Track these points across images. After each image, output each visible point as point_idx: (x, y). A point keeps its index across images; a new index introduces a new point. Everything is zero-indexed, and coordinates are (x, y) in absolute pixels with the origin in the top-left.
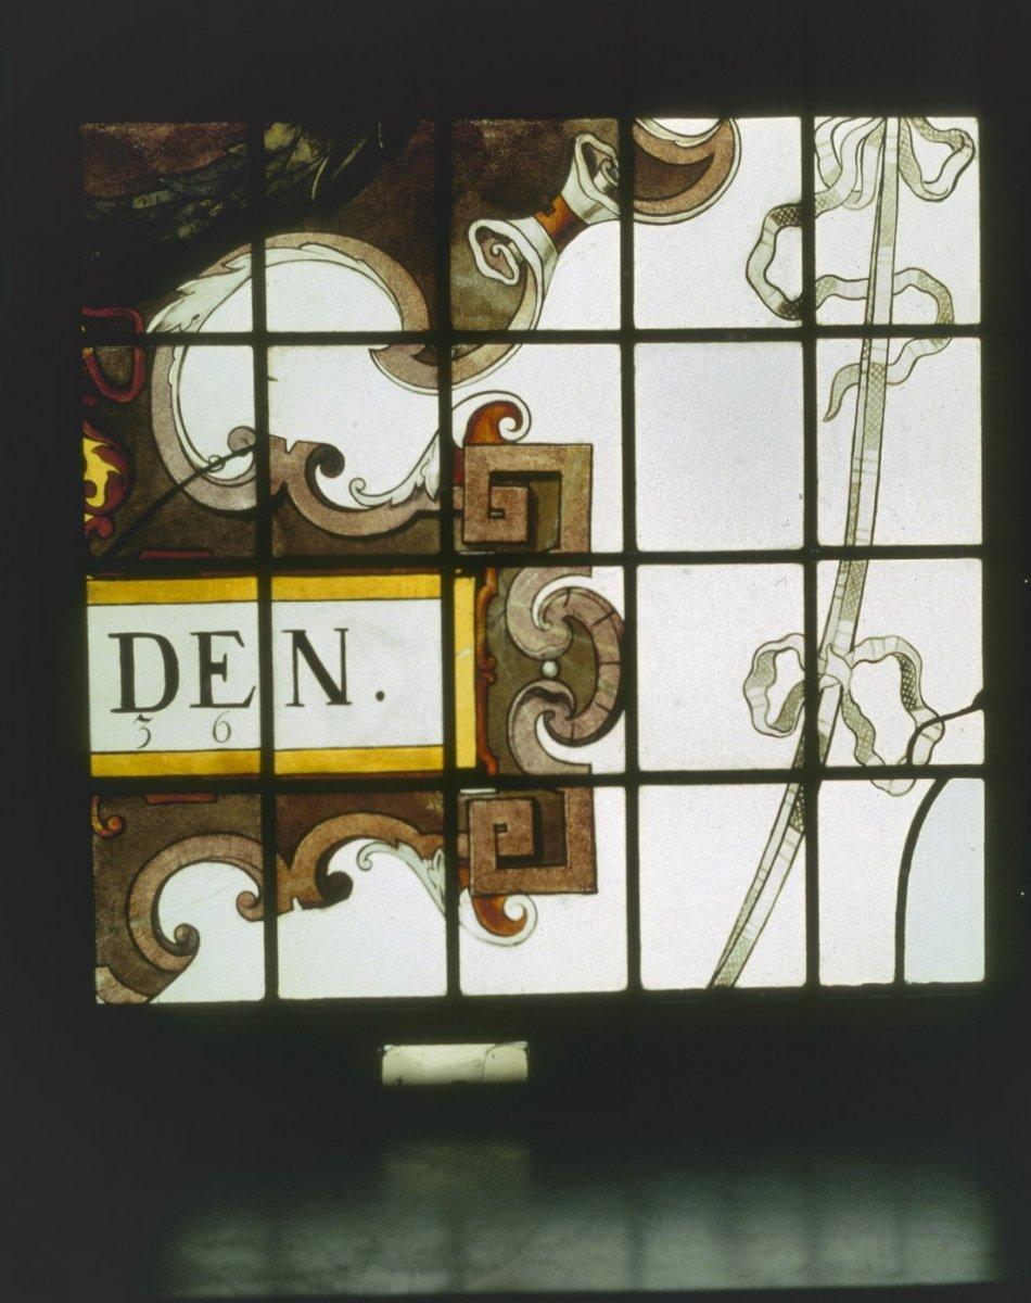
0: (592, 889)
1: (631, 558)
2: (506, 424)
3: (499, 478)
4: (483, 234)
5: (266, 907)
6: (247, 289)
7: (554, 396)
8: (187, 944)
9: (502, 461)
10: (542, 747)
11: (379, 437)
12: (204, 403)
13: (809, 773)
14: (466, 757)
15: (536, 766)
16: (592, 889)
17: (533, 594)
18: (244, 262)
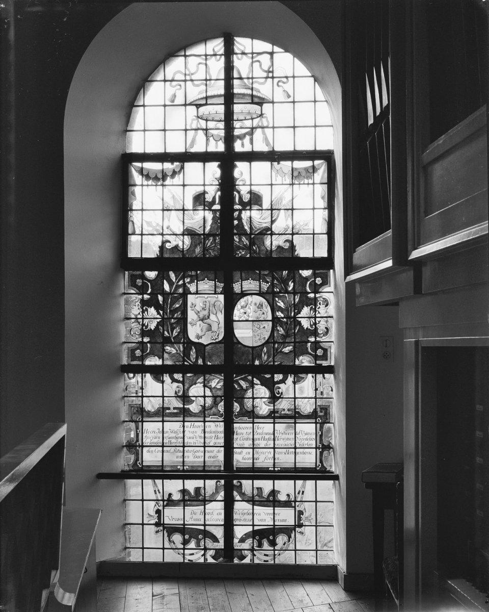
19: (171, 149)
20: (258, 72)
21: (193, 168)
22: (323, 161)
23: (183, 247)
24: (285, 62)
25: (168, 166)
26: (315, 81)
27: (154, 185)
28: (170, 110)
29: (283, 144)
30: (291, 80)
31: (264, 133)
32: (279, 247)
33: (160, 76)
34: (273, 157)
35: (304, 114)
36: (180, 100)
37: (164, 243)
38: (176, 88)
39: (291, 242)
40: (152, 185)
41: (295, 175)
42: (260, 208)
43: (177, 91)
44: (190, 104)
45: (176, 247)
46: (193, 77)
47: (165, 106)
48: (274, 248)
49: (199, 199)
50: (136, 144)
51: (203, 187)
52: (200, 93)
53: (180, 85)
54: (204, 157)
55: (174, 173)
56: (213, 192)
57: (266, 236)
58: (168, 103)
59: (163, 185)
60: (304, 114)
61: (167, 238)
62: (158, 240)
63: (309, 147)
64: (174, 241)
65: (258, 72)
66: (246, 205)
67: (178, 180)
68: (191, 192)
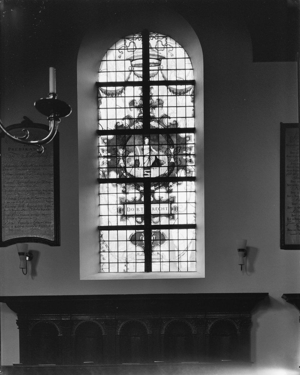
10: (173, 212)
12: (157, 196)
17: (173, 205)
19: (119, 80)
21: (129, 90)
22: (191, 86)
23: (125, 125)
25: (119, 88)
26: (185, 51)
28: (118, 62)
29: (172, 77)
31: (161, 73)
32: (170, 123)
34: (167, 83)
35: (181, 64)
36: (123, 58)
37: (117, 123)
38: (121, 53)
39: (176, 122)
40: (110, 97)
41: (177, 94)
44: (127, 60)
45: (123, 125)
46: (128, 48)
47: (116, 60)
50: (102, 78)
51: (133, 98)
52: (132, 54)
54: (134, 84)
55: (121, 92)
56: (138, 101)
58: (118, 59)
59: (116, 97)
61: (118, 121)
64: (121, 122)
67: (123, 95)
68: (128, 100)
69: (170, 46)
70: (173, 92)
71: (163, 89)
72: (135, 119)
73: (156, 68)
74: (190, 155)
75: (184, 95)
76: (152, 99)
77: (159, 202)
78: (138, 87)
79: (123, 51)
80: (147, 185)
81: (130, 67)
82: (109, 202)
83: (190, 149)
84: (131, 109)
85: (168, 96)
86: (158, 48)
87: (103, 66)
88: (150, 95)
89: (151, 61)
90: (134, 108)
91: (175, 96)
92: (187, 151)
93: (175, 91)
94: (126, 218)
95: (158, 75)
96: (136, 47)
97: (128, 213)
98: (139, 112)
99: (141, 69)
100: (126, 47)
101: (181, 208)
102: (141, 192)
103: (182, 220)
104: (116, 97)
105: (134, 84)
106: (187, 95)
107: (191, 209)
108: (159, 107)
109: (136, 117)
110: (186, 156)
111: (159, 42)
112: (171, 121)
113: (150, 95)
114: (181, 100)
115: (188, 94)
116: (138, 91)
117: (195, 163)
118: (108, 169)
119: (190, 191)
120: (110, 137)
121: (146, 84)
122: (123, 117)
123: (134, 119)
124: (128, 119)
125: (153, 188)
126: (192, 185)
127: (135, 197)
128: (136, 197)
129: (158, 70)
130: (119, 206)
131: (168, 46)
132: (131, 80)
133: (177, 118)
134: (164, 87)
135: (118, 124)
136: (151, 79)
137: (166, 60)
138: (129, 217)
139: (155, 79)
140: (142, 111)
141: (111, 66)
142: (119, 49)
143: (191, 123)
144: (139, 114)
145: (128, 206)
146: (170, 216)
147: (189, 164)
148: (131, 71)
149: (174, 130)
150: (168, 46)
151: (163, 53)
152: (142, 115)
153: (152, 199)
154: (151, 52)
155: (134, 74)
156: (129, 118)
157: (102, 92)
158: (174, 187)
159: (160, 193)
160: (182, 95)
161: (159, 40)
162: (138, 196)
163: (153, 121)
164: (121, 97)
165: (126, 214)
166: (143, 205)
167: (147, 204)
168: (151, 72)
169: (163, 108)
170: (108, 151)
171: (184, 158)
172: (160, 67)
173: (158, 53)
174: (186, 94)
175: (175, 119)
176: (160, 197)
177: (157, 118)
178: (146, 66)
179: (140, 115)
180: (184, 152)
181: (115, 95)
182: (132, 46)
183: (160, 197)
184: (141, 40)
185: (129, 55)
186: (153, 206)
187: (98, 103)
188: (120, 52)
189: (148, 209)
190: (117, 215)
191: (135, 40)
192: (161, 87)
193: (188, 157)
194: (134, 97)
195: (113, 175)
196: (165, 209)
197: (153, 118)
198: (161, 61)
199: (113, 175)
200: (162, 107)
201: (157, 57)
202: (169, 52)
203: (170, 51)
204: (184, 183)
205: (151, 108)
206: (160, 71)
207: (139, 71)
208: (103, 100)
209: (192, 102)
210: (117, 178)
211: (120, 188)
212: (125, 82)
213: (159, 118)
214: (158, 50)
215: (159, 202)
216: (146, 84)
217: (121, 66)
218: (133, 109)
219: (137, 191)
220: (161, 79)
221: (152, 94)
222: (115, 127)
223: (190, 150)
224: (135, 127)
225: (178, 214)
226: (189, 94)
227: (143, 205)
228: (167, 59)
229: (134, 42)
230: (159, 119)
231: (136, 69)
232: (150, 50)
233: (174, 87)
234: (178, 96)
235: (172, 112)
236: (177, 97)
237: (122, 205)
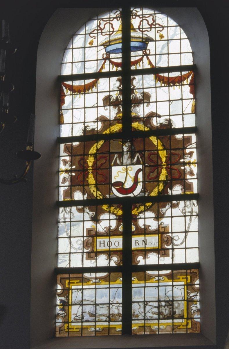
0: (169, 256)
1: (172, 233)
2: (163, 224)
3: (162, 227)
4: (161, 210)
5: (145, 258)
6: (144, 215)
7: (166, 221)
8: (139, 261)
9: (163, 226)
11: (153, 225)
13: (186, 248)
14: (160, 248)
15: (164, 248)
16: (169, 256)
18: (144, 213)
20: (145, 25)
21: (103, 84)
24: (162, 19)
25: (88, 81)
27: (78, 94)
30: (166, 29)
31: (148, 58)
32: (161, 124)
33: (83, 32)
34: (155, 71)
37: (85, 127)
38: (92, 38)
39: (170, 120)
41: (170, 82)
42: (148, 101)
43: (94, 40)
45: (93, 130)
48: (158, 125)
49: (108, 101)
50: (66, 71)
52: (106, 39)
53: (95, 37)
57: (152, 118)
60: (174, 46)
61: (86, 124)
62: (82, 126)
63: (178, 64)
64: (92, 126)
65: (145, 25)
66: (138, 102)
68: (102, 96)
69: (159, 24)
70: (164, 83)
71: (150, 79)
72: (112, 120)
73: (141, 53)
74: (189, 163)
75: (179, 85)
76: (134, 93)
77: (145, 231)
78: (116, 78)
79: (96, 35)
80: (128, 210)
81: (105, 54)
82: (73, 238)
83: (191, 154)
84: (106, 107)
85: (156, 87)
86: (143, 28)
87: (68, 58)
88: (131, 88)
89: (132, 44)
90: (110, 106)
91: (167, 86)
92: (186, 159)
93: (166, 80)
94: (96, 256)
95: (143, 62)
96: (113, 29)
97: (99, 248)
98: (116, 111)
99: (120, 55)
100: (99, 30)
101: (176, 241)
102: (119, 219)
103: (179, 257)
104: (85, 94)
105: (109, 75)
106: (184, 85)
107: (193, 240)
108: (144, 103)
109: (112, 118)
110: (184, 166)
111: (145, 21)
112: (162, 120)
113: (131, 88)
114: (175, 91)
115: (185, 82)
116: (115, 83)
117: (197, 174)
118: (71, 188)
119: (190, 214)
120: (75, 144)
121: (126, 74)
122: (94, 118)
123: (110, 120)
124: (101, 121)
125: (134, 212)
126: (193, 206)
127: (110, 226)
128: (111, 227)
129: (143, 56)
130: (85, 238)
131: (157, 26)
132: (106, 69)
133: (170, 115)
134: (152, 76)
135: (88, 128)
136: (133, 68)
137: (154, 42)
138: (99, 255)
139: (139, 67)
140: (121, 109)
141: (78, 55)
142: (90, 34)
143: (190, 121)
144: (117, 114)
145: (99, 239)
146: (161, 251)
147: (188, 177)
148: (105, 59)
149: (166, 131)
150: (157, 26)
151: (151, 34)
152: (121, 115)
153: (134, 228)
154: (133, 34)
155: (111, 62)
156: (102, 119)
157: (66, 88)
158: (167, 211)
159: (147, 219)
160: (177, 86)
161: (144, 18)
162: (114, 224)
163: (136, 122)
164: (92, 93)
165: (95, 250)
166: (122, 237)
167: (127, 235)
168: (133, 59)
169: (151, 104)
170: (72, 163)
171: (182, 168)
172: (146, 52)
173: (143, 34)
174: (183, 84)
175: (168, 117)
176: (145, 225)
177: (142, 118)
178: (126, 50)
179: (118, 115)
180: (182, 160)
181: (85, 90)
182: (107, 28)
183: (145, 225)
184: (119, 20)
185: (102, 39)
186: (134, 239)
187: (61, 101)
188: (91, 37)
189: (127, 242)
190: (83, 253)
191: (112, 21)
192: (146, 76)
193: (187, 167)
194: (110, 91)
195: (78, 196)
196: (153, 241)
197: (137, 119)
198: (147, 44)
199: (78, 196)
200: (149, 102)
201: (140, 40)
202: (158, 32)
203: (159, 32)
204: (182, 203)
205: (133, 105)
206: (145, 57)
207: (117, 58)
208: (68, 99)
209: (191, 92)
210: (84, 200)
211: (88, 214)
212: (97, 73)
213: (144, 118)
214: (143, 32)
215: (145, 231)
216: (126, 74)
217: (91, 53)
218: (108, 107)
219: (113, 217)
220: (147, 66)
221: (135, 86)
222: (83, 132)
223: (190, 157)
224: (111, 130)
225: (173, 249)
226: (187, 83)
227: (122, 237)
228: (155, 41)
229: (110, 23)
230: (145, 119)
231: (112, 56)
232: (132, 31)
233: (166, 75)
234: (171, 86)
235: (163, 109)
236: (170, 87)
237: (91, 238)
